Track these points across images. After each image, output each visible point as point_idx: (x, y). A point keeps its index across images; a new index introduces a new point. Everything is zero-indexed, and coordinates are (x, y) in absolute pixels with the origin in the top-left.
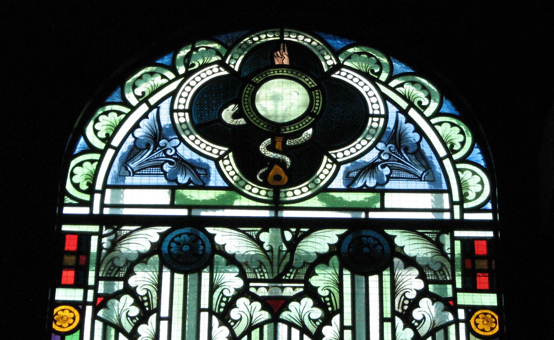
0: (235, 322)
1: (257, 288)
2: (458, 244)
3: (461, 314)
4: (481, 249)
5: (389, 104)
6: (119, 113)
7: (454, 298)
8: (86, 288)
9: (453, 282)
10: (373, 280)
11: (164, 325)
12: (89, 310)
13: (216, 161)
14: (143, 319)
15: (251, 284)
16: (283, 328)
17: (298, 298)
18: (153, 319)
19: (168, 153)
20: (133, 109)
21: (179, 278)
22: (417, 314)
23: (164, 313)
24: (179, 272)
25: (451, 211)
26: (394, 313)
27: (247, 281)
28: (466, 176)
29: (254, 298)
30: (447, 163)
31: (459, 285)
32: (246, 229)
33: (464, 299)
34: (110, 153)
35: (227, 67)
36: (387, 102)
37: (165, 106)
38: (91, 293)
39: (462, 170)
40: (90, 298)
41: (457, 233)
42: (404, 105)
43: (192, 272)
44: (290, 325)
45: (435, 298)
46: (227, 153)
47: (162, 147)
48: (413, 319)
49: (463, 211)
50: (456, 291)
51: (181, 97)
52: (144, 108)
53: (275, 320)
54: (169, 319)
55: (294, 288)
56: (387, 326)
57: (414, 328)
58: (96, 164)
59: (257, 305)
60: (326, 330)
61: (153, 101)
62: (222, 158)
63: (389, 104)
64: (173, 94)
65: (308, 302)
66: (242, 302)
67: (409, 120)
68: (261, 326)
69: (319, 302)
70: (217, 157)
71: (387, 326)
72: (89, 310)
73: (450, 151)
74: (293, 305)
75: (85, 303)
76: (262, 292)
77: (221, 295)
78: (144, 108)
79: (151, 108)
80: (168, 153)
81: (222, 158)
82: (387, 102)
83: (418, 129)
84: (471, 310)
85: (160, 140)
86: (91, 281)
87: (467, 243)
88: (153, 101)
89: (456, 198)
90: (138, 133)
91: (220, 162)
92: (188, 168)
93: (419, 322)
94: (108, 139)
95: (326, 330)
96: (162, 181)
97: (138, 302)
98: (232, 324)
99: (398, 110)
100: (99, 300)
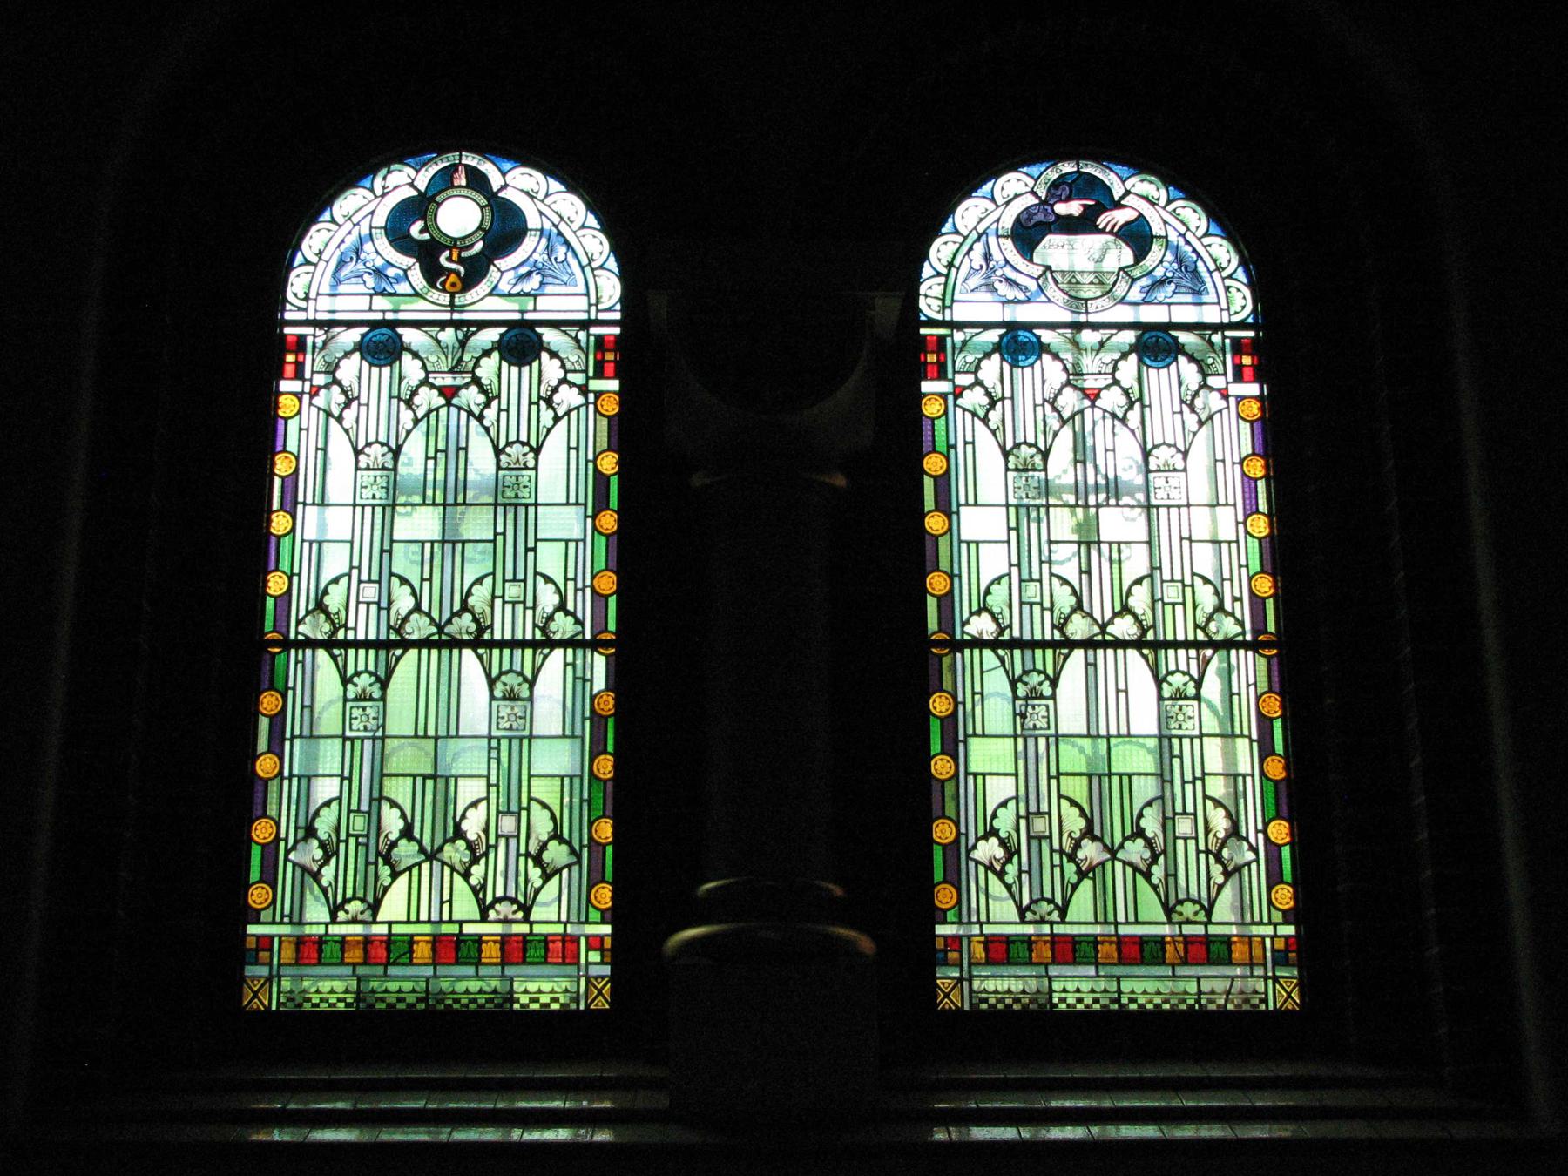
3: (591, 397)
6: (329, 230)
7: (586, 385)
8: (304, 380)
10: (526, 369)
11: (363, 409)
12: (306, 398)
14: (347, 405)
18: (355, 404)
19: (368, 265)
23: (363, 400)
25: (588, 312)
26: (540, 398)
27: (428, 373)
29: (433, 386)
30: (587, 270)
31: (591, 373)
34: (322, 264)
35: (415, 188)
38: (307, 384)
39: (599, 276)
40: (307, 389)
44: (460, 408)
49: (598, 311)
56: (534, 408)
59: (435, 392)
60: (486, 412)
61: (355, 219)
64: (372, 213)
65: (474, 389)
66: (424, 390)
69: (483, 390)
71: (534, 408)
72: (306, 398)
73: (591, 260)
74: (463, 392)
75: (303, 393)
76: (438, 382)
80: (368, 265)
84: (598, 394)
86: (307, 375)
87: (600, 340)
89: (593, 301)
90: (343, 247)
93: (558, 405)
94: (320, 254)
96: (362, 289)
97: (344, 392)
100: (314, 390)
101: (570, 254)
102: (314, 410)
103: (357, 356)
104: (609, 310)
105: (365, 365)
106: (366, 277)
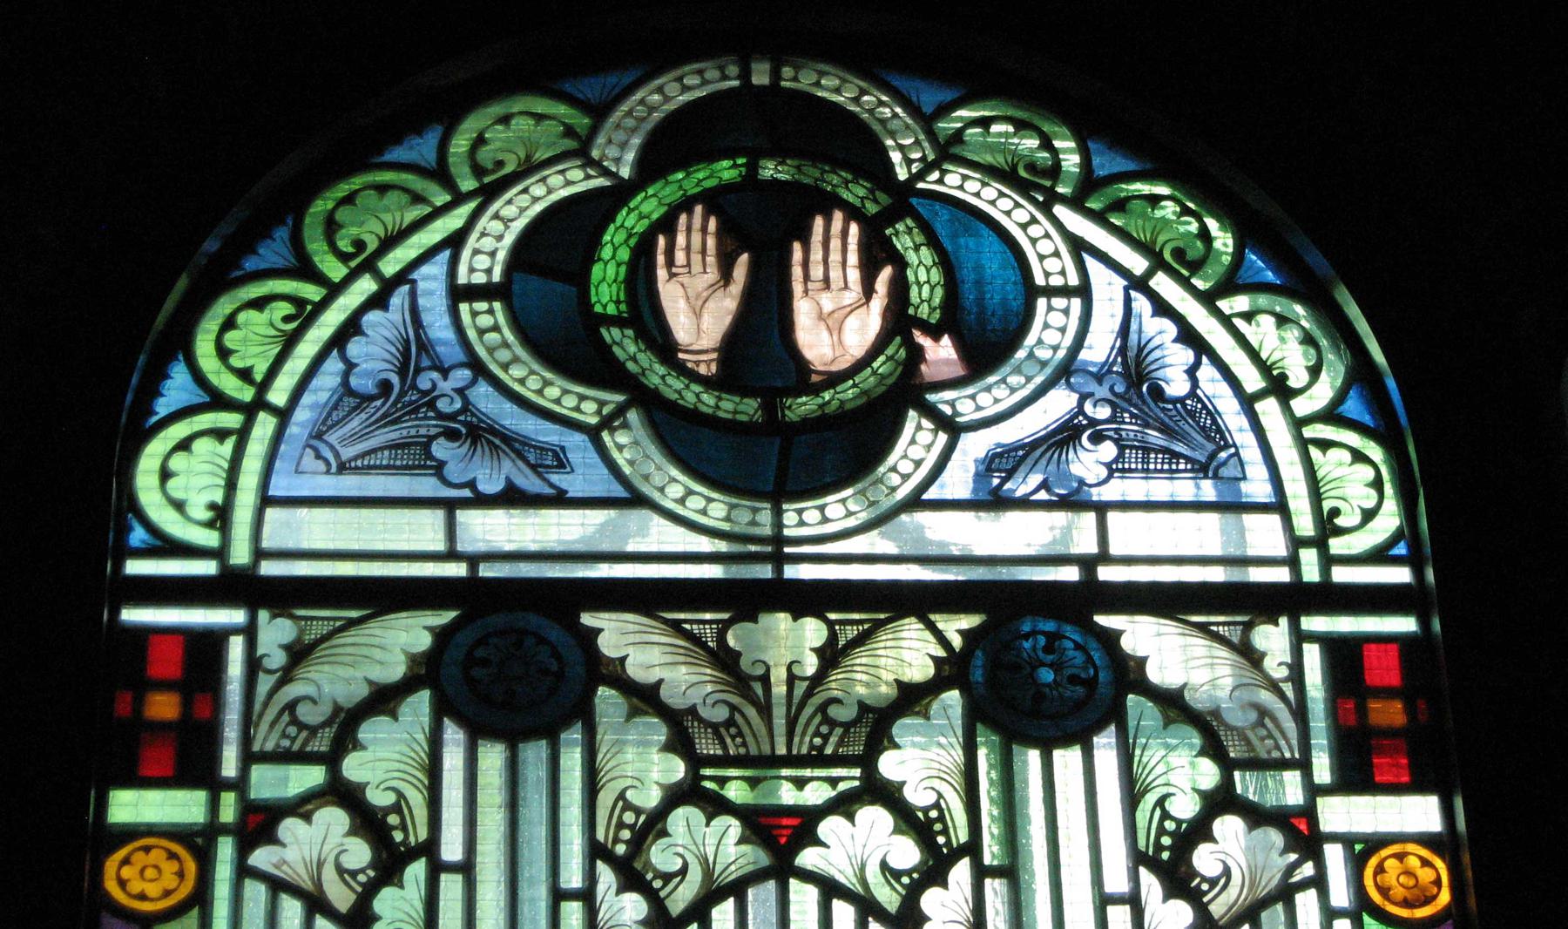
0: (667, 877)
1: (722, 781)
2: (1312, 655)
3: (1334, 855)
4: (1383, 670)
5: (1090, 262)
8: (213, 784)
9: (1304, 765)
11: (451, 886)
12: (226, 849)
13: (594, 433)
15: (708, 772)
16: (804, 897)
17: (844, 805)
19: (442, 405)
20: (335, 290)
21: (492, 757)
22: (1205, 859)
23: (452, 850)
24: (494, 734)
25: (1293, 562)
27: (696, 762)
28: (1331, 464)
29: (716, 806)
32: (682, 616)
33: (1339, 814)
36: (1086, 257)
37: (431, 278)
38: (229, 800)
40: (228, 811)
41: (1314, 623)
42: (1137, 264)
43: (531, 734)
45: (1256, 816)
46: (621, 411)
47: (425, 393)
48: (1195, 874)
49: (1328, 561)
50: (1314, 791)
51: (476, 252)
52: (366, 286)
53: (782, 870)
54: (467, 868)
55: (833, 782)
57: (1194, 898)
58: (228, 446)
60: (931, 900)
61: (390, 265)
62: (607, 423)
63: (1090, 262)
66: (684, 819)
67: (1162, 308)
68: (738, 889)
70: (594, 420)
72: (226, 849)
74: (830, 827)
75: (212, 830)
77: (620, 804)
78: (366, 286)
79: (388, 287)
80: (442, 405)
81: (607, 423)
82: (1086, 257)
83: (1189, 336)
84: (1363, 849)
85: (418, 371)
86: (229, 767)
87: (1341, 652)
88: (390, 265)
89: (1305, 525)
91: (605, 436)
92: (504, 452)
93: (1213, 882)
95: (931, 900)
98: (657, 884)
99: (1126, 283)
100: (255, 820)
101: (1207, 372)
102: (256, 892)
103: (420, 705)
104: (1379, 556)
105: (454, 736)
106: (440, 449)
